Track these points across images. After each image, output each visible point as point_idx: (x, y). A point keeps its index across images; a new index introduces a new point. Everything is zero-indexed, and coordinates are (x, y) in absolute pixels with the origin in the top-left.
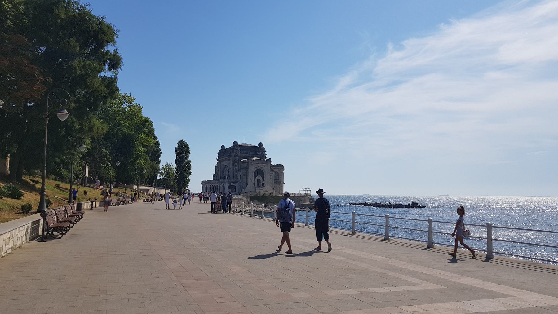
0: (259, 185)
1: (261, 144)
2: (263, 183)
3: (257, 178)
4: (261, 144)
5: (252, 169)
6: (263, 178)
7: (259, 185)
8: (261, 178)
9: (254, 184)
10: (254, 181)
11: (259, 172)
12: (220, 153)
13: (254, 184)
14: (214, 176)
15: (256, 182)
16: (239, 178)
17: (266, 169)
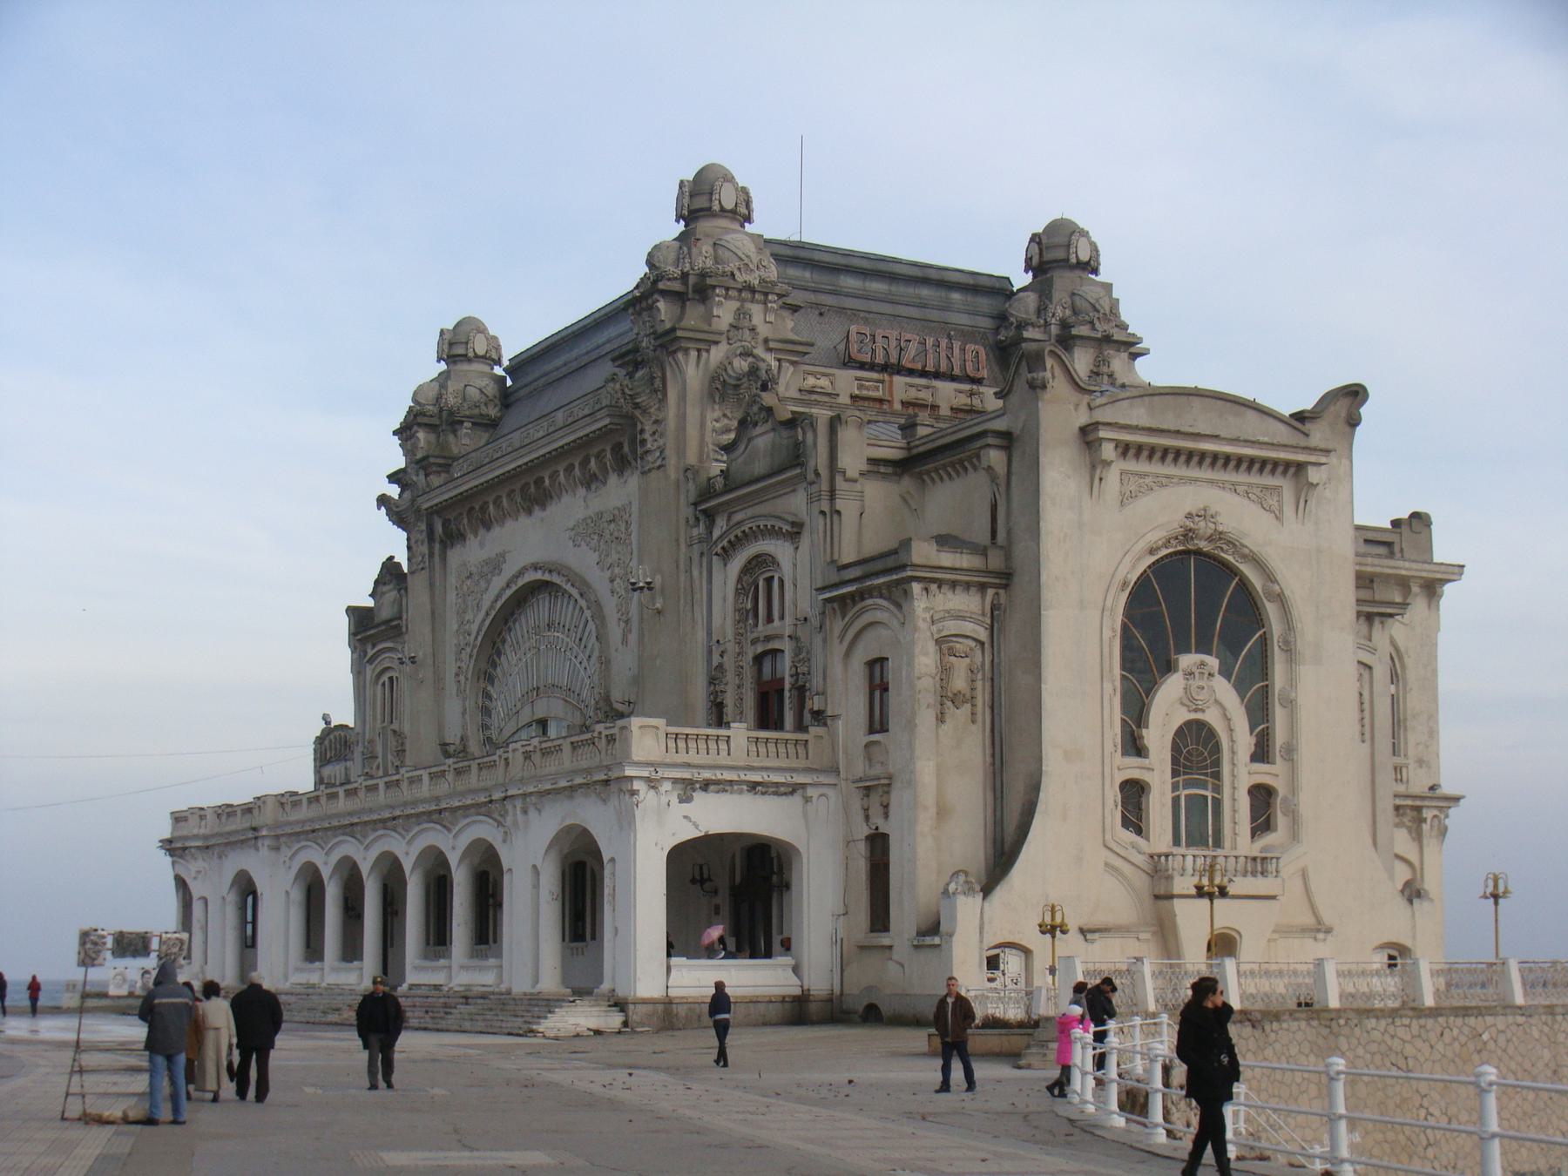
0: (1199, 825)
1: (1058, 254)
2: (1262, 796)
3: (1168, 707)
4: (1058, 254)
5: (1092, 540)
6: (1259, 711)
7: (1199, 825)
8: (1224, 706)
9: (1134, 793)
10: (1134, 745)
11: (1195, 605)
12: (426, 424)
13: (1134, 793)
14: (332, 746)
15: (1157, 771)
16: (846, 698)
17: (1297, 555)
